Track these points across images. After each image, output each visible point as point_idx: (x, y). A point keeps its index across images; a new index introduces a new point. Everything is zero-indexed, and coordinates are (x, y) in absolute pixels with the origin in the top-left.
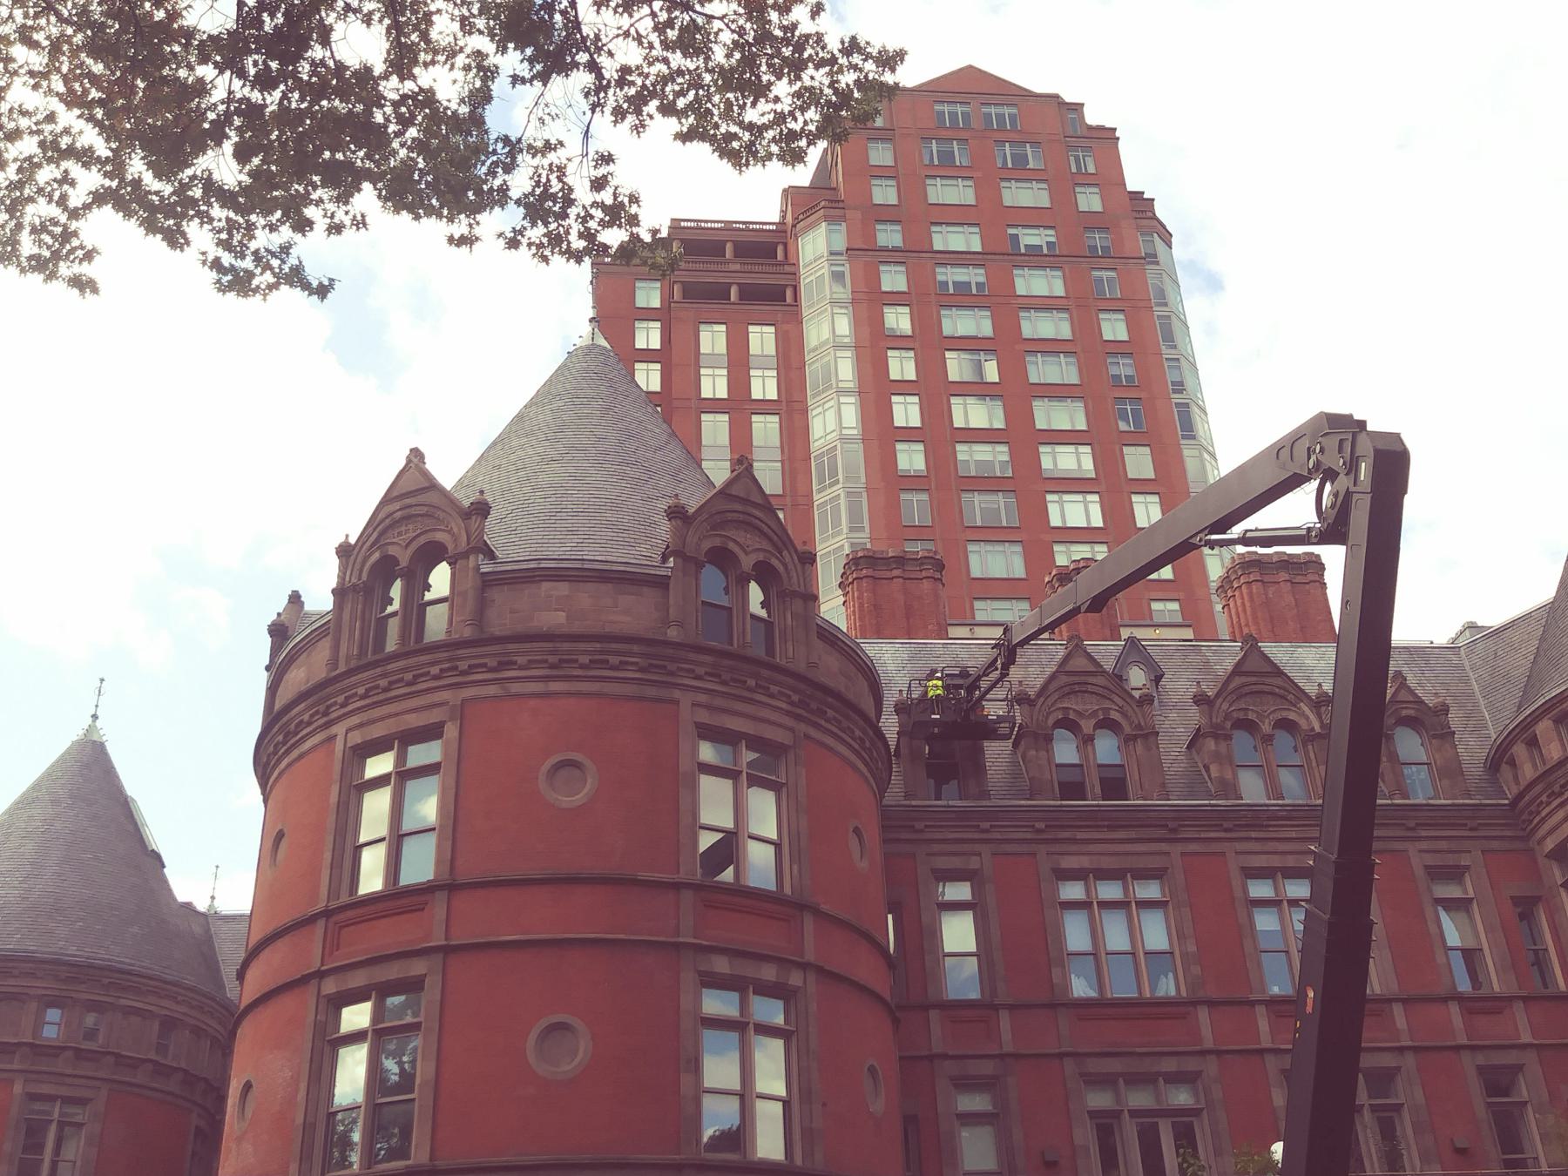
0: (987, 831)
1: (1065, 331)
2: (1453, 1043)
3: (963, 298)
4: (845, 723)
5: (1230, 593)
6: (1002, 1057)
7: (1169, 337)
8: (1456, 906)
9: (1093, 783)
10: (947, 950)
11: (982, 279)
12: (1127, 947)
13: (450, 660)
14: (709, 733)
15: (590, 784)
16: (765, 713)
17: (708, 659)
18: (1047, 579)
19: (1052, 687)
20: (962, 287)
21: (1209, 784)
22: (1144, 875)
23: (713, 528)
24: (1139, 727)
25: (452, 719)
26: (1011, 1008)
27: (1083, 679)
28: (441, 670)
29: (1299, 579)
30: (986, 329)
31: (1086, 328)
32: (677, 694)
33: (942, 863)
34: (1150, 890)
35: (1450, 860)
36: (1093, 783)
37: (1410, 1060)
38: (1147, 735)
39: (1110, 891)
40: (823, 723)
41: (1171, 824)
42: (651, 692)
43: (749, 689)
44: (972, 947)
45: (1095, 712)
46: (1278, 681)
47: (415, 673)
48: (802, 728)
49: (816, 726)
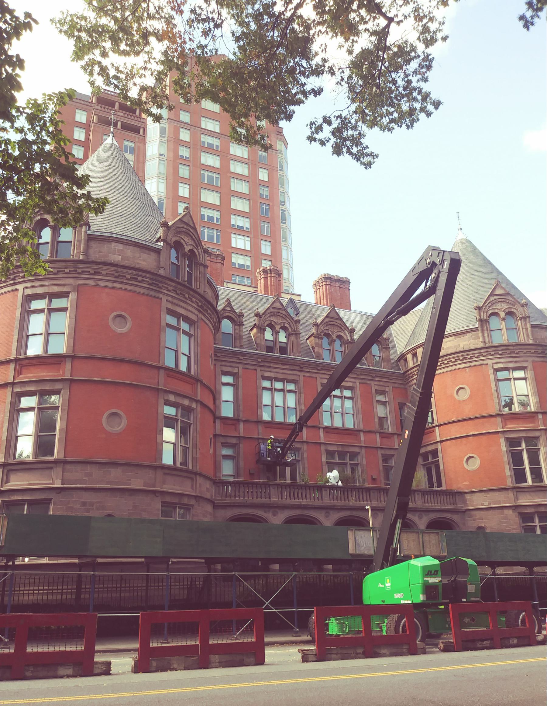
0: (241, 360)
1: (246, 173)
2: (376, 446)
3: (210, 149)
4: (212, 316)
5: (318, 287)
6: (239, 437)
7: (282, 184)
8: (384, 403)
9: (277, 348)
10: (223, 399)
11: (218, 144)
12: (282, 405)
13: (73, 267)
14: (171, 312)
15: (129, 325)
16: (190, 308)
17: (173, 284)
18: (258, 270)
19: (268, 312)
20: (210, 146)
21: (313, 354)
22: (290, 381)
23: (176, 234)
24: (294, 331)
25: (74, 291)
26: (244, 421)
27: (278, 311)
28: (70, 271)
29: (342, 286)
30: (217, 164)
31: (254, 173)
32: (161, 296)
33: (225, 369)
34: (292, 387)
35: (383, 388)
36: (277, 348)
37: (363, 450)
38: (298, 334)
39: (278, 385)
40: (206, 314)
41: (301, 366)
42: (152, 293)
43: (186, 298)
44: (231, 399)
45: (280, 323)
46: (340, 322)
47: (58, 270)
48: (200, 315)
49: (204, 315)
